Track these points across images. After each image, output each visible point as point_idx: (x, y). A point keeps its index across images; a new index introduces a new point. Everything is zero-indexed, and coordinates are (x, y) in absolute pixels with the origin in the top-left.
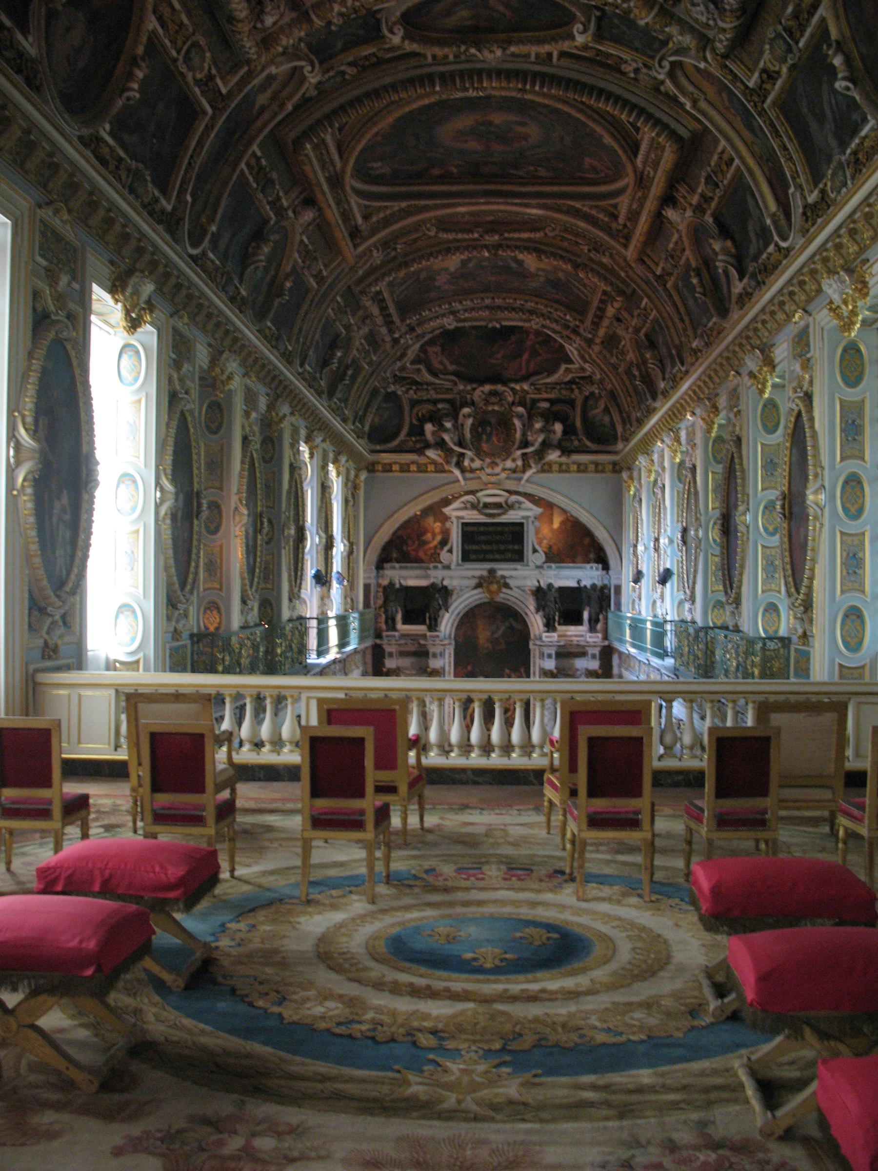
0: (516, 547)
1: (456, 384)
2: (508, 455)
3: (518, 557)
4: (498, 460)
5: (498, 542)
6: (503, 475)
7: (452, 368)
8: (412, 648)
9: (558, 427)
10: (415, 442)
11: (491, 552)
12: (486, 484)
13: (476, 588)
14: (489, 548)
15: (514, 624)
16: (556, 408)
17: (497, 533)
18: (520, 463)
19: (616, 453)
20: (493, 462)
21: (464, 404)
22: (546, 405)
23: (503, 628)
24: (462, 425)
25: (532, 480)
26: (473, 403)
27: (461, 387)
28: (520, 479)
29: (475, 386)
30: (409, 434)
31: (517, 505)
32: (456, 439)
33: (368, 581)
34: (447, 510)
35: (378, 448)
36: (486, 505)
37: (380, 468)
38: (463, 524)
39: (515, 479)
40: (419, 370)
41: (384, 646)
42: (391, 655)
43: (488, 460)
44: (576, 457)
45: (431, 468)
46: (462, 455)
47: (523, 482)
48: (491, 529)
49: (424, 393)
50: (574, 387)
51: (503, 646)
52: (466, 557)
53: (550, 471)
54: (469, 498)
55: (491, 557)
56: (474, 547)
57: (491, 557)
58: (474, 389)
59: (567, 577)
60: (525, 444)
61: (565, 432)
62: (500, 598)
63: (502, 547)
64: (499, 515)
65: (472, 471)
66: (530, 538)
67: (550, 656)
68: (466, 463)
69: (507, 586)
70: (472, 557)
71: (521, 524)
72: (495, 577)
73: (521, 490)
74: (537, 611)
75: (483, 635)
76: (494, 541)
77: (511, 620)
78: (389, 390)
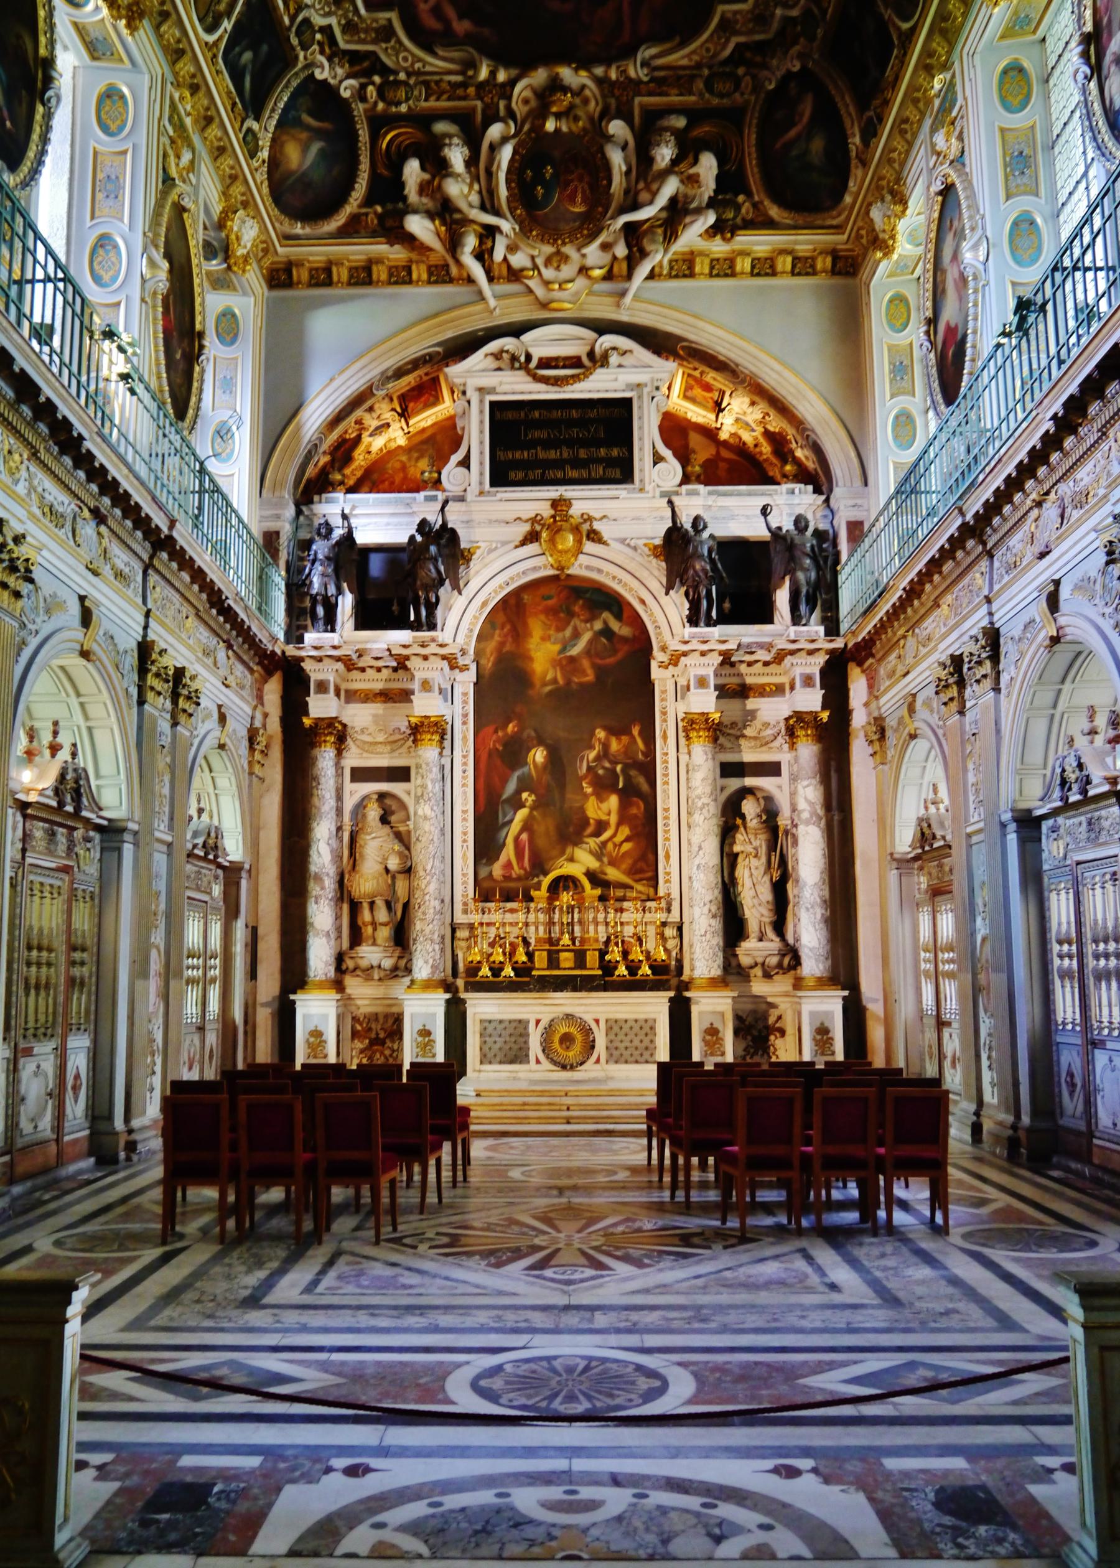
0: (615, 452)
1: (474, 65)
2: (593, 236)
3: (622, 472)
4: (569, 250)
5: (570, 443)
6: (581, 282)
7: (462, 26)
8: (373, 682)
9: (708, 166)
10: (380, 217)
11: (559, 464)
12: (544, 305)
13: (523, 543)
14: (552, 455)
15: (615, 625)
16: (703, 130)
17: (571, 423)
18: (621, 251)
19: (839, 228)
20: (558, 253)
21: (491, 118)
22: (681, 122)
23: (586, 637)
24: (489, 174)
25: (647, 300)
26: (511, 114)
27: (484, 73)
28: (623, 294)
29: (514, 72)
30: (368, 201)
31: (614, 359)
32: (475, 198)
33: (272, 526)
34: (456, 371)
35: (298, 229)
36: (545, 363)
37: (305, 276)
38: (493, 405)
39: (610, 294)
40: (386, 33)
41: (307, 665)
42: (322, 687)
43: (548, 249)
44: (745, 240)
45: (419, 272)
46: (490, 232)
47: (628, 299)
48: (557, 414)
49: (402, 93)
50: (741, 71)
51: (590, 677)
52: (500, 477)
53: (691, 275)
54: (507, 343)
55: (560, 475)
56: (518, 455)
57: (560, 475)
58: (512, 83)
59: (738, 514)
60: (635, 206)
61: (719, 179)
62: (580, 567)
63: (583, 454)
64: (576, 378)
65: (515, 275)
66: (646, 432)
67: (702, 682)
68: (499, 255)
69: (594, 536)
70: (512, 475)
71: (627, 403)
72: (567, 518)
73: (624, 317)
74: (669, 588)
75: (543, 653)
76: (562, 442)
77: (606, 615)
78: (319, 75)
